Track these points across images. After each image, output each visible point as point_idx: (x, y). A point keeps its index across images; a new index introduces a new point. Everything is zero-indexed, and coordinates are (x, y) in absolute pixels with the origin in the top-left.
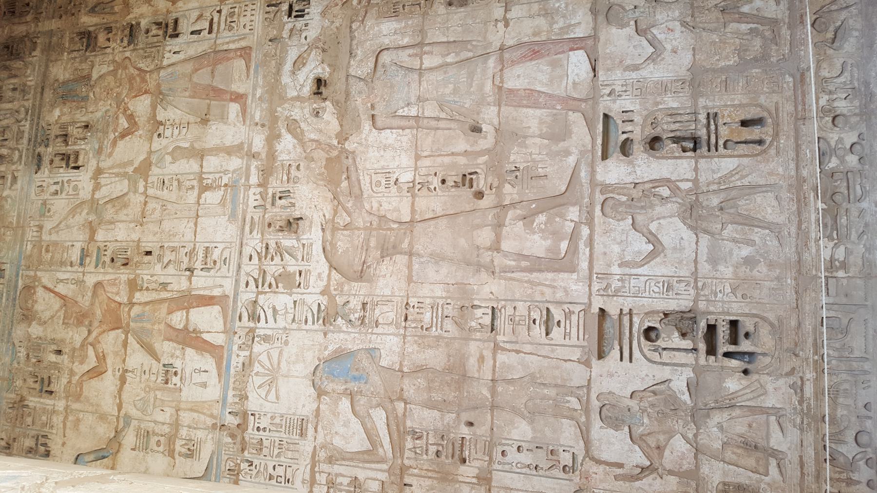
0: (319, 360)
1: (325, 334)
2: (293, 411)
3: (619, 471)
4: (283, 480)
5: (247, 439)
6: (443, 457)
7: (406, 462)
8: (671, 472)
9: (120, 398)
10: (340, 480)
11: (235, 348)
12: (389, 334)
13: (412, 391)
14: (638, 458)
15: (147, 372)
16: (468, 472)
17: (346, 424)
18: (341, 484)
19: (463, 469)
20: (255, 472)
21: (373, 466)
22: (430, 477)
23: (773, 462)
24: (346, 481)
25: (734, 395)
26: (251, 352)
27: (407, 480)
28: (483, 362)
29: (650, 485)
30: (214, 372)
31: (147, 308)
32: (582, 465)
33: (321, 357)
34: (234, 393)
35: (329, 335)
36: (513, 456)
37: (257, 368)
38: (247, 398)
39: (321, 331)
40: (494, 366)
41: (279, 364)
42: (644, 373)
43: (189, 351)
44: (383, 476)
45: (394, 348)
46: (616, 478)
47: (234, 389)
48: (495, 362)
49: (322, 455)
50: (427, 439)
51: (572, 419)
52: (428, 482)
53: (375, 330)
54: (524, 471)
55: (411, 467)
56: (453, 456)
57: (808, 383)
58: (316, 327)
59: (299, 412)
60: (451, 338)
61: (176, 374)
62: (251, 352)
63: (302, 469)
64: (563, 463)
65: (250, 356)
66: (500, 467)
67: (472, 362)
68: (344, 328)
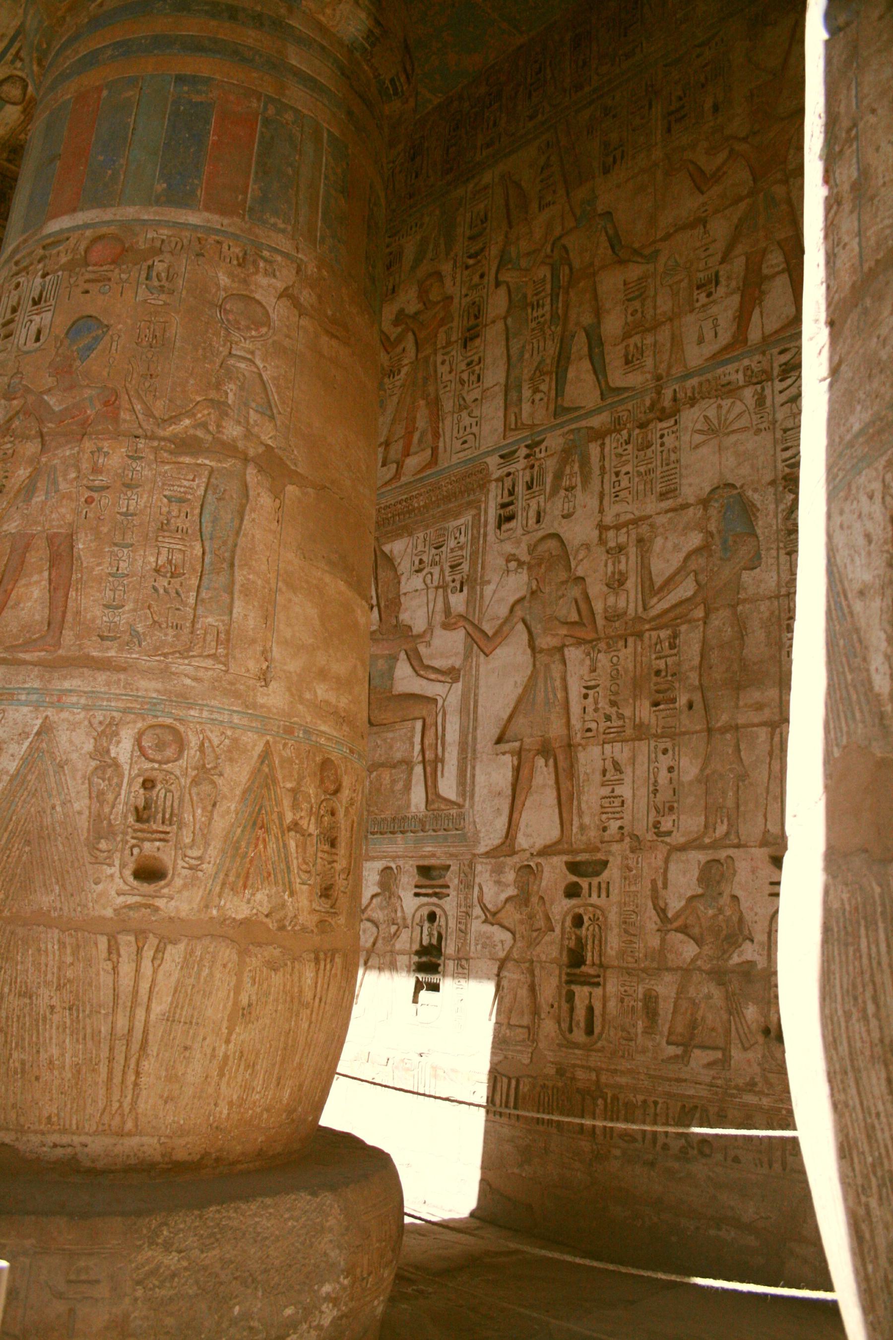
0: (742, 487)
1: (773, 483)
2: (684, 472)
3: (660, 884)
4: (617, 489)
5: (650, 427)
6: (654, 679)
7: (647, 634)
8: (663, 940)
9: (676, 231)
10: (623, 559)
11: (746, 362)
12: (778, 573)
13: (717, 623)
14: (675, 905)
15: (707, 253)
16: (644, 711)
17: (676, 548)
18: (619, 562)
19: (647, 704)
20: (620, 451)
21: (640, 596)
22: (635, 667)
23: (679, 1051)
24: (623, 567)
25: (741, 1015)
26: (744, 386)
27: (631, 640)
28: (757, 710)
29: (650, 918)
30: (716, 347)
31: (784, 207)
32: (662, 842)
33: (746, 487)
34: (696, 385)
35: (771, 490)
36: (665, 761)
37: (726, 403)
38: (692, 406)
39: (776, 476)
40: (754, 725)
41: (733, 432)
42: (759, 910)
43: (736, 298)
44: (631, 612)
45: (762, 585)
46: (654, 882)
47: (701, 384)
48: (757, 725)
49: (644, 529)
50: (671, 656)
51: (706, 827)
52: (630, 666)
53: (782, 552)
54: (652, 776)
55: (642, 641)
56: (658, 692)
57: (757, 1098)
58: (780, 465)
59: (684, 481)
60: (780, 661)
61: (709, 295)
62: (744, 386)
63: (629, 508)
64: (662, 820)
65: (740, 388)
66: (652, 748)
67: (756, 695)
68: (782, 507)
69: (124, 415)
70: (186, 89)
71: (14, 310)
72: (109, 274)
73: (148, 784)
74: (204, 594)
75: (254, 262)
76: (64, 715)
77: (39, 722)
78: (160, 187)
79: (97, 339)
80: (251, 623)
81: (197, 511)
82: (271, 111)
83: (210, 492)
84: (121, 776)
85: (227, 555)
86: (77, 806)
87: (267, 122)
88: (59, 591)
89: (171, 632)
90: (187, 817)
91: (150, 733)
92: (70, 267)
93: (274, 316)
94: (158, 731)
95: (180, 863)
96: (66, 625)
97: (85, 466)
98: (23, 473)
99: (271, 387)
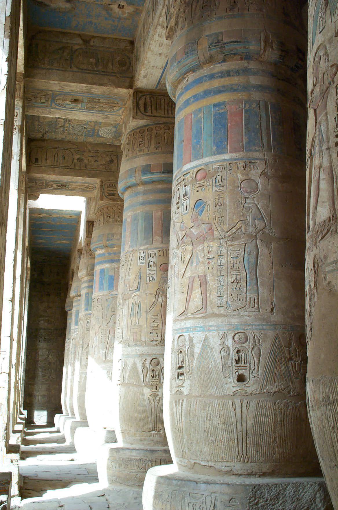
69: (215, 233)
70: (217, 109)
71: (179, 198)
72: (203, 184)
73: (238, 352)
74: (248, 288)
75: (250, 166)
76: (211, 333)
77: (204, 336)
78: (214, 148)
79: (203, 207)
80: (266, 294)
81: (242, 261)
82: (247, 106)
83: (246, 253)
84: (230, 351)
85: (254, 273)
86: (218, 362)
87: (246, 111)
88: (204, 294)
89: (240, 302)
90: (252, 361)
91: (237, 335)
92: (192, 183)
93: (259, 184)
94: (239, 334)
95: (251, 376)
96: (208, 305)
97: (206, 252)
98: (189, 256)
99: (262, 211)
